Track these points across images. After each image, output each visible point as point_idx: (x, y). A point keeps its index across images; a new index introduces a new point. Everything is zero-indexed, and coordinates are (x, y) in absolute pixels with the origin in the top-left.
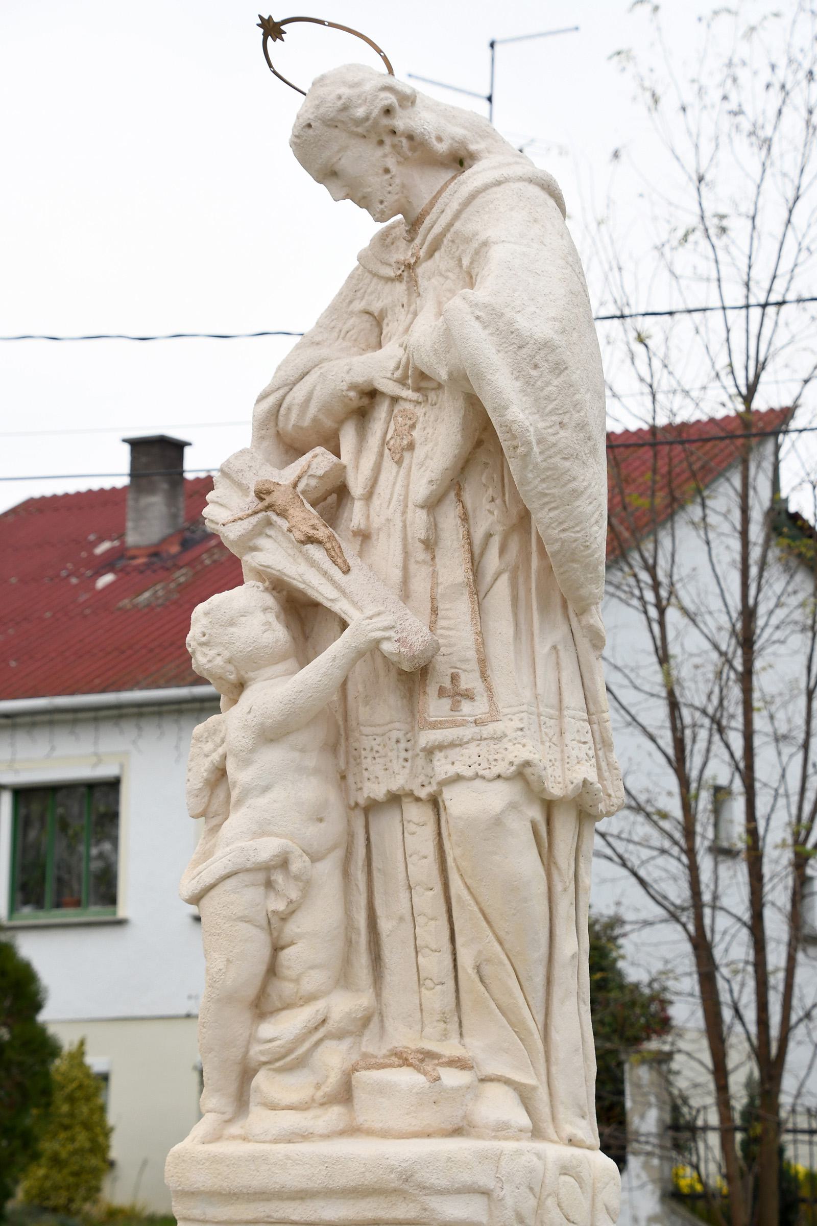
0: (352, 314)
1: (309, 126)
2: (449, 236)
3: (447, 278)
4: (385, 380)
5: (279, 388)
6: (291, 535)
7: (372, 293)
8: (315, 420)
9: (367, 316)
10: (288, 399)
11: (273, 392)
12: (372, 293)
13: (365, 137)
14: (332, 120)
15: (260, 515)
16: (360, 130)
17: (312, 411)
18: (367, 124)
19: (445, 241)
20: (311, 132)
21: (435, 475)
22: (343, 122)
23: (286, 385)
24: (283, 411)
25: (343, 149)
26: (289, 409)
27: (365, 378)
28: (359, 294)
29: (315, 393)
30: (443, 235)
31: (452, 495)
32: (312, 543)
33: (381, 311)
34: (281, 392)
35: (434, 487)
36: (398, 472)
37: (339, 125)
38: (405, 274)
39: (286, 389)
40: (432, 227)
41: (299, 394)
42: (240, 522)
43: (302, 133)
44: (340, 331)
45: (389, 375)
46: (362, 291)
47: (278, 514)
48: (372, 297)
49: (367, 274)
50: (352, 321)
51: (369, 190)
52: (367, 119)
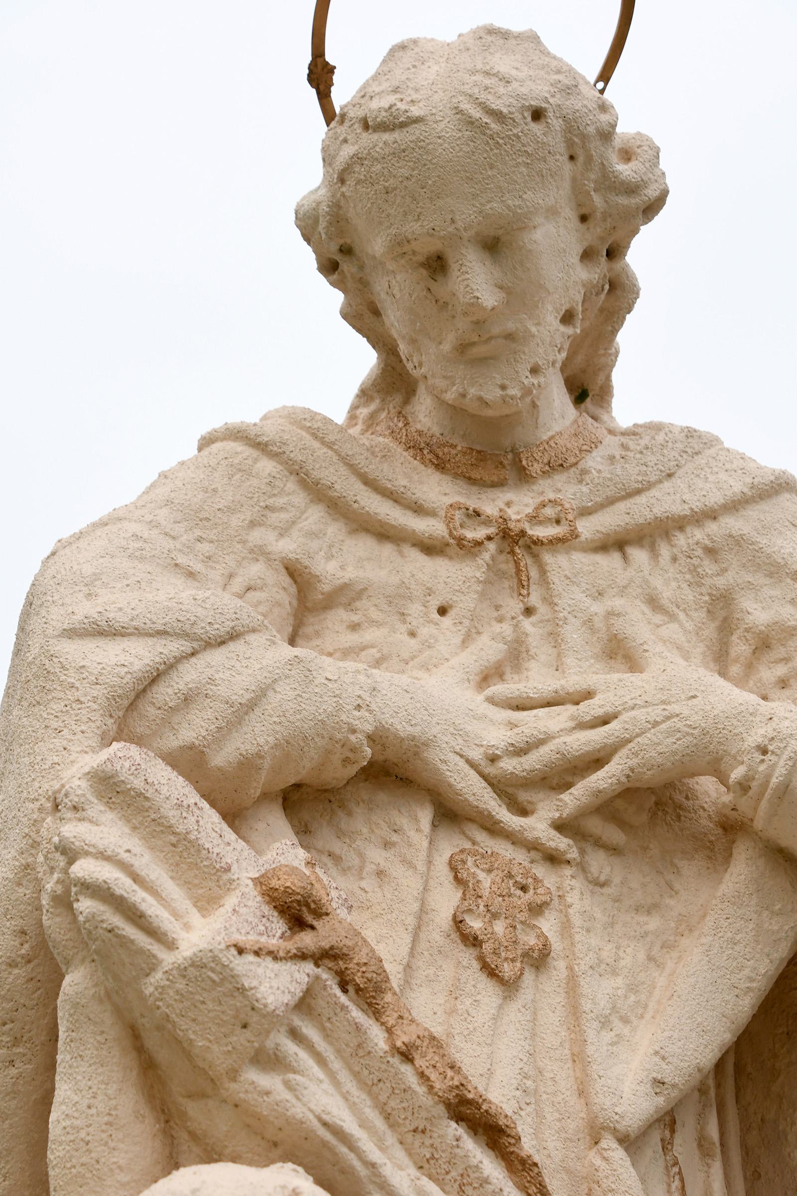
0: (260, 553)
1: (537, 115)
2: (698, 534)
3: (672, 617)
4: (462, 763)
5: (162, 633)
6: (406, 1070)
7: (313, 535)
8: (247, 765)
9: (286, 580)
10: (189, 675)
11: (140, 633)
12: (313, 535)
13: (584, 219)
14: (584, 137)
15: (309, 967)
16: (597, 200)
17: (257, 736)
18: (623, 200)
19: (681, 540)
20: (536, 128)
21: (669, 1073)
22: (589, 159)
23: (185, 635)
24: (165, 693)
25: (552, 212)
26: (187, 699)
27: (416, 731)
28: (274, 518)
29: (274, 699)
30: (680, 523)
31: (656, 1137)
32: (459, 1118)
33: (343, 588)
34: (173, 647)
35: (661, 1100)
36: (500, 1007)
37: (581, 159)
38: (492, 546)
39: (185, 646)
40: (638, 492)
41: (231, 672)
42: (268, 961)
43: (517, 116)
44: (231, 576)
45: (476, 755)
46: (283, 516)
47: (344, 986)
48: (314, 545)
49: (291, 485)
50: (256, 570)
51: (534, 329)
52: (631, 189)
